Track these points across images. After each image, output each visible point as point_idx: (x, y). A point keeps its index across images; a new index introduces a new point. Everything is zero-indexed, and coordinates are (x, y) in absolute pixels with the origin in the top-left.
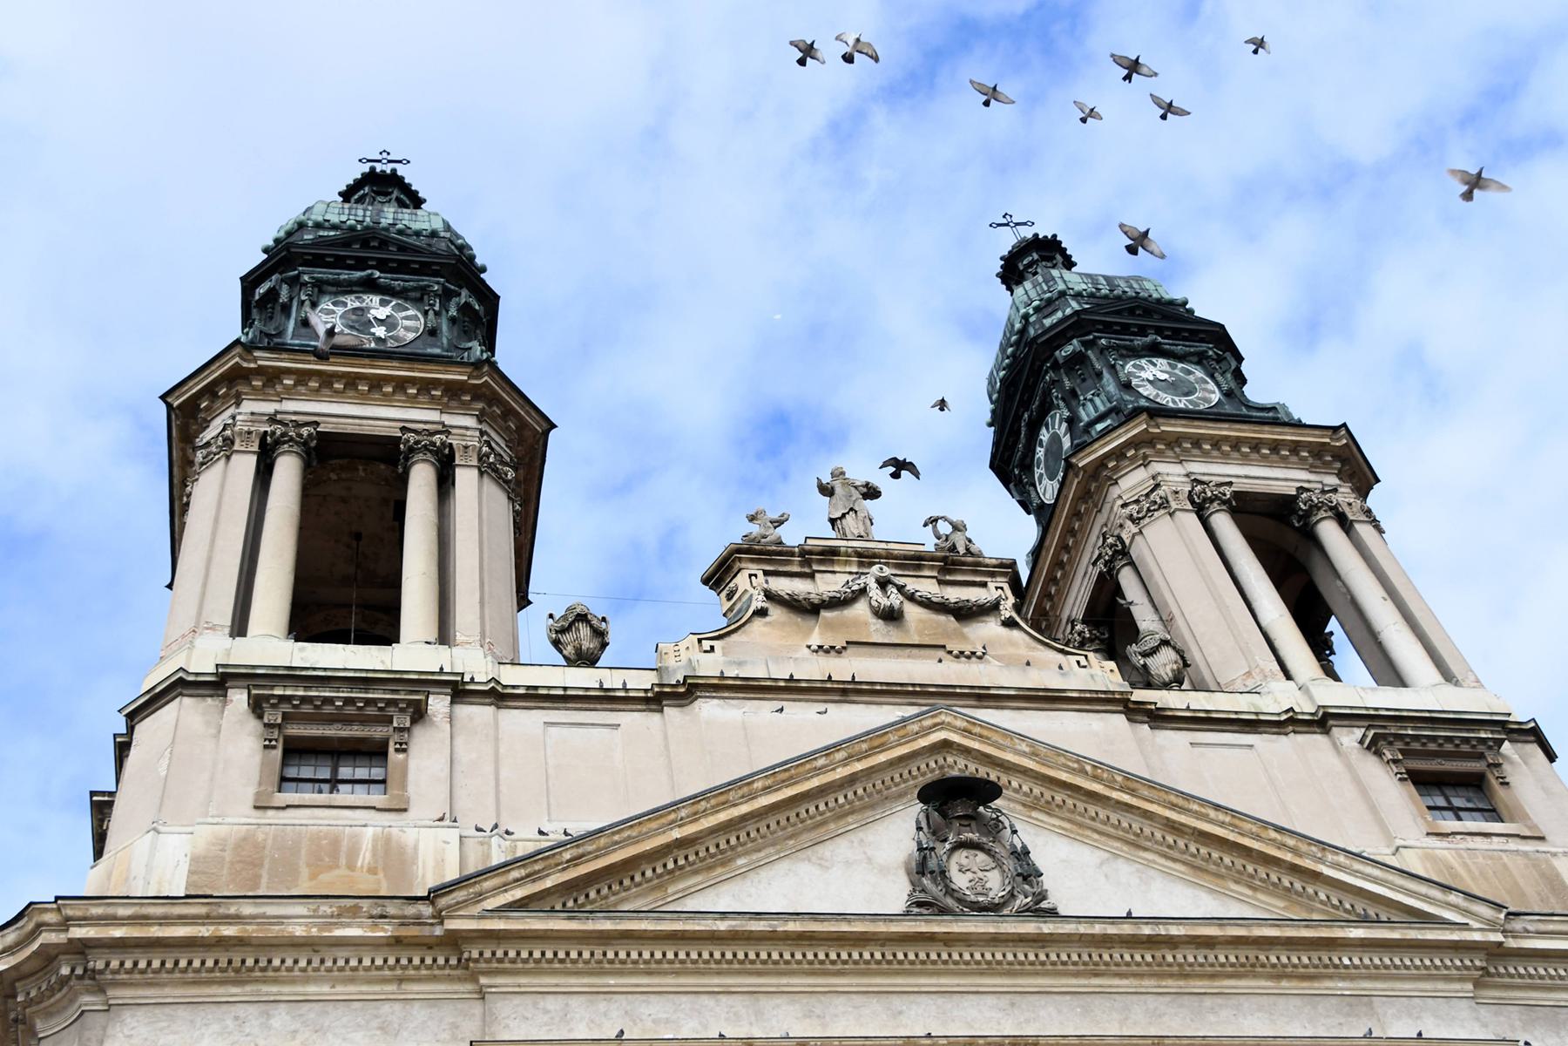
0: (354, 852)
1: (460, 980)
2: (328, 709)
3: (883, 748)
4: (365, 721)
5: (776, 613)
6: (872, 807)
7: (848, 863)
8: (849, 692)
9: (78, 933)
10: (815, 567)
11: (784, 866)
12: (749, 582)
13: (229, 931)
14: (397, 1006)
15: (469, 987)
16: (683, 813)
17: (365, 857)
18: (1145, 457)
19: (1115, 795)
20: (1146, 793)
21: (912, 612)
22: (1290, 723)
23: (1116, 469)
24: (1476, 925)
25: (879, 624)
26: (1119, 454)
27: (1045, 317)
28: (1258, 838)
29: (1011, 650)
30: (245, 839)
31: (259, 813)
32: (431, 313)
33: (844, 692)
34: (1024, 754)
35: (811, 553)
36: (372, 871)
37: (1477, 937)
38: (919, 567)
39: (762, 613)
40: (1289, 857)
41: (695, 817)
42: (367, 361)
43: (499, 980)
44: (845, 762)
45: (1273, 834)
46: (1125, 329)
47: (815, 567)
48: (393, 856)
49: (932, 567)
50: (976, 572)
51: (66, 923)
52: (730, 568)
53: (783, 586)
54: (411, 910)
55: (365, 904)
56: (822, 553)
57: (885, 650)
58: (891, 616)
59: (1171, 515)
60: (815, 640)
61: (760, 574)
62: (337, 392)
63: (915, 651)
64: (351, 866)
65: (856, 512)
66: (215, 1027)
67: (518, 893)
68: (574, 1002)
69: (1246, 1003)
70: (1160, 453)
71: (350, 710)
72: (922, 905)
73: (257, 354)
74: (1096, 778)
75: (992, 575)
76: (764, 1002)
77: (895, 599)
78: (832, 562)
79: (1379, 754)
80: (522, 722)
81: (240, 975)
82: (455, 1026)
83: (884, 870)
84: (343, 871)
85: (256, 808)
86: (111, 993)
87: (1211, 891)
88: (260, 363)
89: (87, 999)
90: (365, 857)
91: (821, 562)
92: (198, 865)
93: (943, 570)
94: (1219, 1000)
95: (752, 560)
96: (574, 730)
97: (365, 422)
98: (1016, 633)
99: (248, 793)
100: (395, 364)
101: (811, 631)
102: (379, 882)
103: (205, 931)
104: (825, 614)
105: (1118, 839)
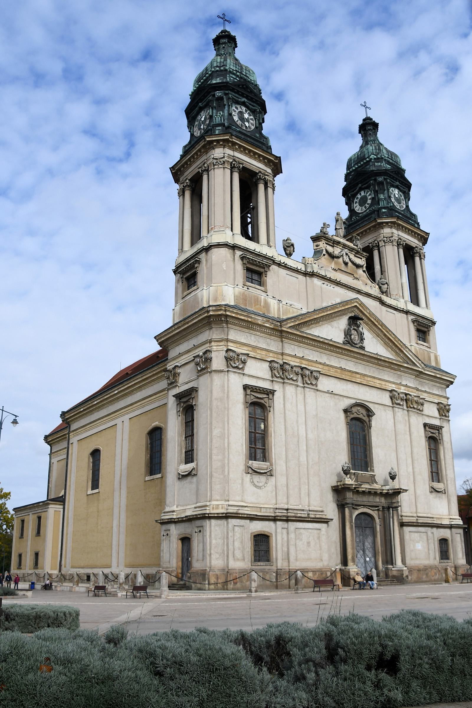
1: (279, 338)
2: (255, 263)
4: (260, 267)
5: (327, 256)
6: (341, 316)
7: (336, 328)
8: (338, 283)
9: (228, 313)
10: (335, 245)
11: (326, 325)
12: (322, 244)
13: (250, 320)
14: (269, 340)
15: (279, 339)
17: (262, 304)
18: (392, 226)
19: (379, 326)
20: (384, 327)
21: (350, 264)
23: (385, 226)
25: (343, 265)
26: (387, 223)
27: (376, 162)
28: (397, 342)
33: (337, 283)
34: (367, 313)
35: (335, 242)
36: (264, 307)
37: (420, 370)
38: (352, 251)
39: (324, 255)
40: (400, 347)
42: (255, 147)
43: (285, 340)
45: (400, 342)
47: (335, 245)
49: (354, 252)
50: (361, 255)
51: (225, 311)
52: (319, 239)
53: (330, 249)
54: (277, 323)
55: (271, 320)
56: (337, 242)
57: (344, 273)
58: (346, 264)
59: (393, 245)
62: (246, 153)
63: (348, 274)
64: (260, 305)
66: (244, 337)
68: (296, 347)
69: (386, 372)
70: (395, 227)
71: (258, 264)
73: (233, 137)
74: (377, 322)
75: (364, 257)
76: (323, 355)
77: (347, 260)
78: (338, 245)
79: (414, 323)
80: (283, 272)
81: (248, 328)
84: (259, 306)
86: (229, 325)
88: (233, 140)
89: (224, 325)
90: (262, 304)
91: (336, 244)
92: (236, 298)
93: (356, 253)
94: (382, 371)
95: (324, 239)
96: (291, 277)
97: (251, 165)
98: (365, 274)
100: (260, 150)
101: (331, 263)
103: (246, 319)
104: (335, 259)
105: (375, 334)
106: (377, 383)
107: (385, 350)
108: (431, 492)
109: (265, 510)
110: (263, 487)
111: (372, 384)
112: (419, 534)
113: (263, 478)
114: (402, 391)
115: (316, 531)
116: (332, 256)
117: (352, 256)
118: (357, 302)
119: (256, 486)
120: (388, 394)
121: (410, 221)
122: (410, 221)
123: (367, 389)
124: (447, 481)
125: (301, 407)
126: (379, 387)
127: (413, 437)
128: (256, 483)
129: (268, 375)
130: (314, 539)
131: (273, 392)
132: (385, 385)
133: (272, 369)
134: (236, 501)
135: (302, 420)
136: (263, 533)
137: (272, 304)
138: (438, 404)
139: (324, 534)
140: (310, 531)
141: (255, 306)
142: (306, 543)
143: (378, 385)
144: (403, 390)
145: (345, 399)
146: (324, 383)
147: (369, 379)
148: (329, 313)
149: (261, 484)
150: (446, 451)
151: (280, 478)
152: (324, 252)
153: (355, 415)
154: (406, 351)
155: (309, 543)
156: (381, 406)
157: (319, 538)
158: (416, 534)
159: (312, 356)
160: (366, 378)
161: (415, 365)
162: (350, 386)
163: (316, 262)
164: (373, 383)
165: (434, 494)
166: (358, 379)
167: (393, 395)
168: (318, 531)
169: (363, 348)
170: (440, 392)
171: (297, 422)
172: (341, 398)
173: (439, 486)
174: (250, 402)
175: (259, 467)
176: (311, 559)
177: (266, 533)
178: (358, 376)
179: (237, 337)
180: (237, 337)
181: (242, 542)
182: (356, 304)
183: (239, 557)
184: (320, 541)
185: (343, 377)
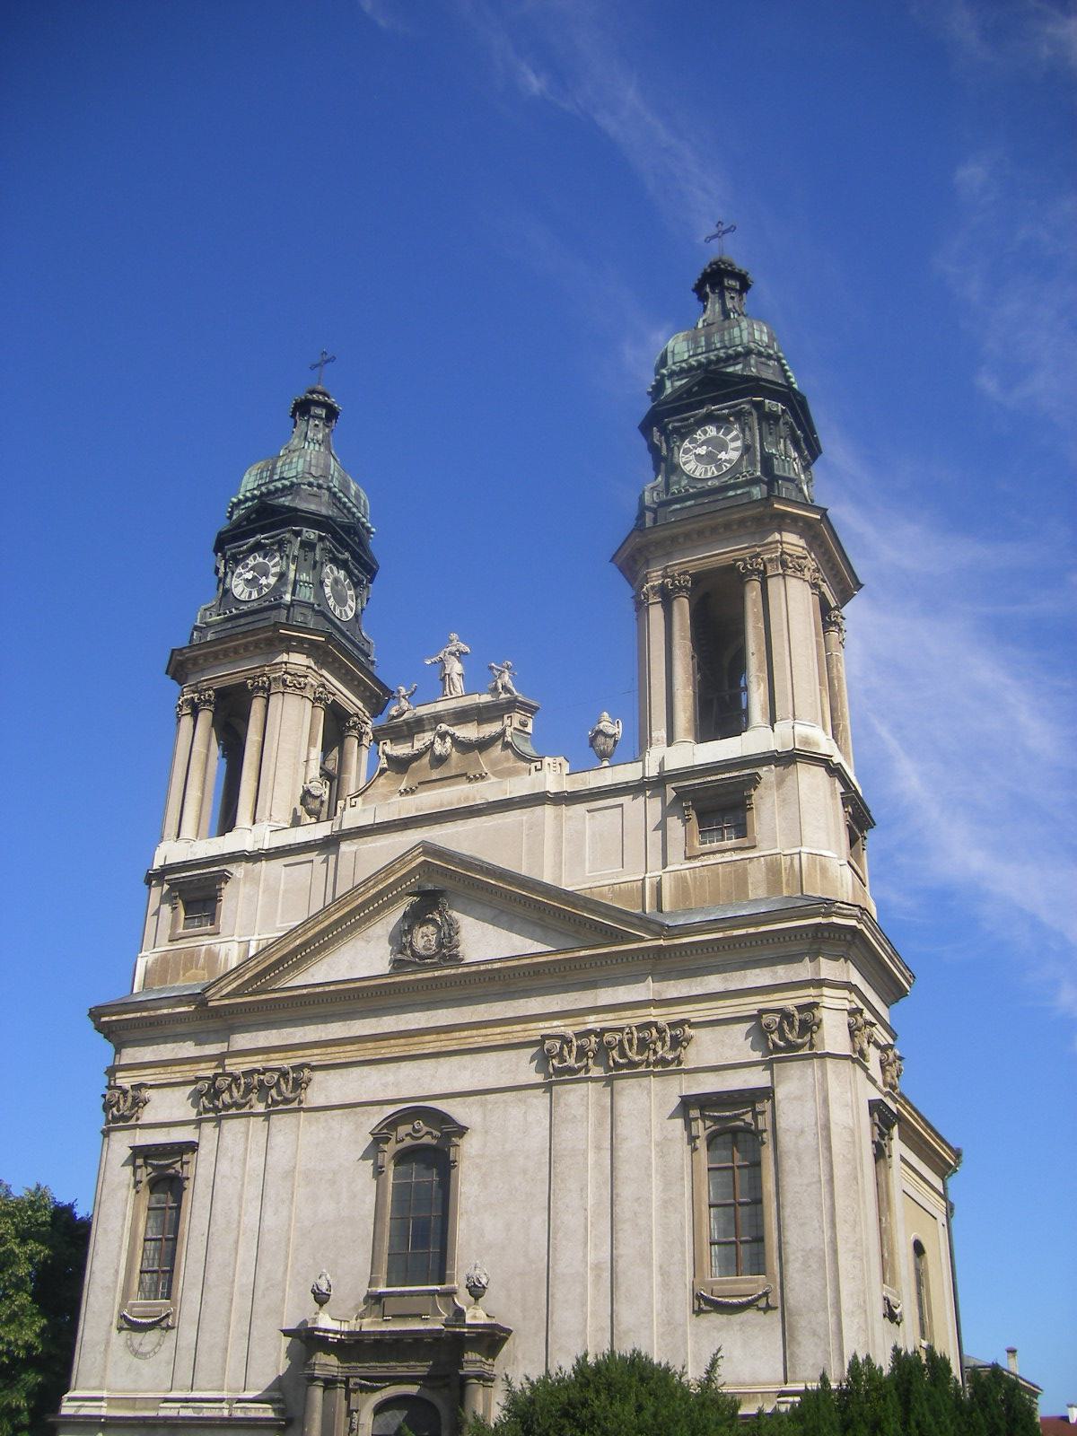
3: (394, 873)
16: (300, 932)
29: (506, 765)
30: (162, 960)
31: (170, 944)
32: (285, 558)
39: (383, 771)
41: (305, 932)
44: (373, 886)
48: (212, 957)
60: (402, 788)
61: (388, 741)
63: (452, 780)
65: (449, 675)
85: (170, 941)
90: (202, 960)
95: (384, 734)
102: (204, 975)
106: (496, 1036)
108: (698, 1312)
110: (151, 1355)
113: (152, 1336)
117: (469, 732)
118: (425, 853)
119: (136, 1353)
121: (731, 493)
122: (731, 493)
123: (467, 1058)
125: (256, 1161)
127: (622, 1153)
131: (192, 1147)
134: (88, 1389)
135: (253, 1191)
141: (184, 975)
143: (499, 1037)
144: (593, 1022)
146: (325, 1088)
148: (336, 917)
149: (144, 1349)
150: (788, 1163)
151: (187, 1332)
152: (384, 763)
153: (408, 1142)
162: (407, 1067)
164: (480, 1039)
165: (716, 1319)
166: (431, 1045)
171: (241, 1198)
172: (376, 1108)
173: (751, 1284)
174: (145, 1179)
175: (143, 1312)
179: (138, 1055)
180: (138, 1055)
182: (423, 858)
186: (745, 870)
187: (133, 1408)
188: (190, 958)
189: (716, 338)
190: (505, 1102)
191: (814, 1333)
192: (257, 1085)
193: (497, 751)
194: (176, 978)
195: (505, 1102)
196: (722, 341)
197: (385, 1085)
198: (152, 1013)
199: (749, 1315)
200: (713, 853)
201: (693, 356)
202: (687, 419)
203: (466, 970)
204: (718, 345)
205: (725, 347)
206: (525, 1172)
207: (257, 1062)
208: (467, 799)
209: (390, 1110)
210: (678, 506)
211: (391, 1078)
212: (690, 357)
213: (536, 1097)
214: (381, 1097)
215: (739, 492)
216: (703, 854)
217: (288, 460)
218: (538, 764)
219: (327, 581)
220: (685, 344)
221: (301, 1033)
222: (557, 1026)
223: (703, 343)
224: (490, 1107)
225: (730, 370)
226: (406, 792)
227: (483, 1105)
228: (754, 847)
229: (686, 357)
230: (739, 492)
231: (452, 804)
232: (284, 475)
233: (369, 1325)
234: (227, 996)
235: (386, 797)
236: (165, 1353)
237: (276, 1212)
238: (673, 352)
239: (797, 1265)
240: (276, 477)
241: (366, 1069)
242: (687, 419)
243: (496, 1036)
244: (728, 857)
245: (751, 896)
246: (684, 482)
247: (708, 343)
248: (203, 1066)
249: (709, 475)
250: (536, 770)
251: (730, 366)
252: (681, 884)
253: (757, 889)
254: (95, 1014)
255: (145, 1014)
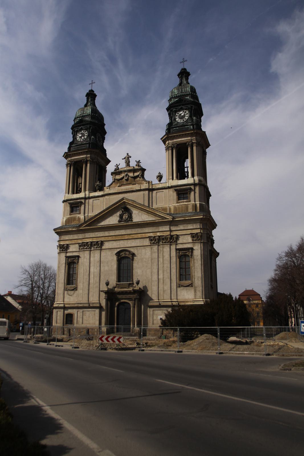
0: (76, 218)
7: (115, 216)
17: (77, 219)
22: (169, 188)
24: (170, 218)
29: (140, 182)
46: (178, 106)
48: (79, 219)
57: (126, 185)
60: (118, 185)
67: (85, 225)
72: (119, 221)
80: (91, 200)
82: (83, 236)
83: (117, 216)
87: (148, 215)
90: (77, 219)
99: (69, 213)
106: (139, 236)
107: (147, 216)
109: (72, 304)
111: (136, 237)
112: (161, 311)
113: (72, 292)
114: (158, 235)
115: (93, 312)
116: (118, 180)
117: (131, 174)
119: (69, 295)
120: (148, 239)
121: (186, 127)
122: (186, 127)
123: (133, 240)
124: (194, 279)
126: (141, 237)
128: (70, 294)
129: (78, 250)
130: (92, 315)
132: (145, 235)
133: (80, 246)
136: (70, 313)
137: (81, 218)
138: (191, 234)
139: (97, 313)
140: (90, 311)
142: (88, 317)
144: (158, 234)
145: (118, 249)
147: (133, 235)
149: (72, 294)
150: (195, 261)
151: (80, 291)
154: (158, 213)
155: (89, 317)
156: (142, 247)
157: (95, 314)
158: (159, 311)
159: (99, 235)
160: (131, 235)
161: (166, 218)
162: (122, 242)
163: (108, 187)
164: (136, 237)
165: (182, 288)
167: (151, 239)
168: (95, 312)
169: (132, 221)
170: (195, 226)
172: (116, 249)
173: (188, 282)
176: (90, 323)
177: (71, 313)
178: (126, 236)
179: (65, 238)
181: (60, 317)
183: (59, 322)
184: (95, 316)
185: (117, 239)
186: (188, 206)
187: (70, 305)
188: (74, 219)
189: (183, 90)
190: (141, 248)
191: (199, 291)
192: (92, 244)
193: (138, 179)
194: (71, 223)
195: (141, 248)
196: (185, 90)
197: (117, 245)
198: (68, 230)
199: (188, 288)
200: (182, 202)
201: (178, 93)
202: (177, 109)
203: (133, 223)
204: (184, 91)
205: (185, 92)
206: (145, 262)
207: (91, 240)
208: (132, 189)
209: (119, 250)
210: (175, 129)
211: (118, 244)
212: (177, 94)
213: (147, 248)
214: (116, 247)
215: (188, 127)
216: (180, 202)
217: (87, 109)
218: (146, 182)
219: (97, 137)
220: (176, 90)
221: (99, 235)
222: (152, 235)
223: (180, 91)
224: (138, 249)
225: (186, 98)
226: (118, 186)
227: (137, 249)
228: (190, 201)
229: (177, 94)
230: (188, 127)
231: (128, 189)
232: (87, 112)
233: (116, 289)
234: (84, 227)
235: (114, 187)
236: (75, 295)
237: (96, 269)
238: (174, 92)
239: (196, 279)
240: (85, 113)
241: (113, 242)
242: (177, 109)
243: (139, 236)
244: (184, 203)
245: (189, 211)
246: (176, 123)
247: (182, 91)
248: (79, 240)
249: (181, 122)
250: (146, 183)
251: (186, 97)
252: (175, 207)
253: (190, 210)
254: (55, 230)
255: (66, 230)
